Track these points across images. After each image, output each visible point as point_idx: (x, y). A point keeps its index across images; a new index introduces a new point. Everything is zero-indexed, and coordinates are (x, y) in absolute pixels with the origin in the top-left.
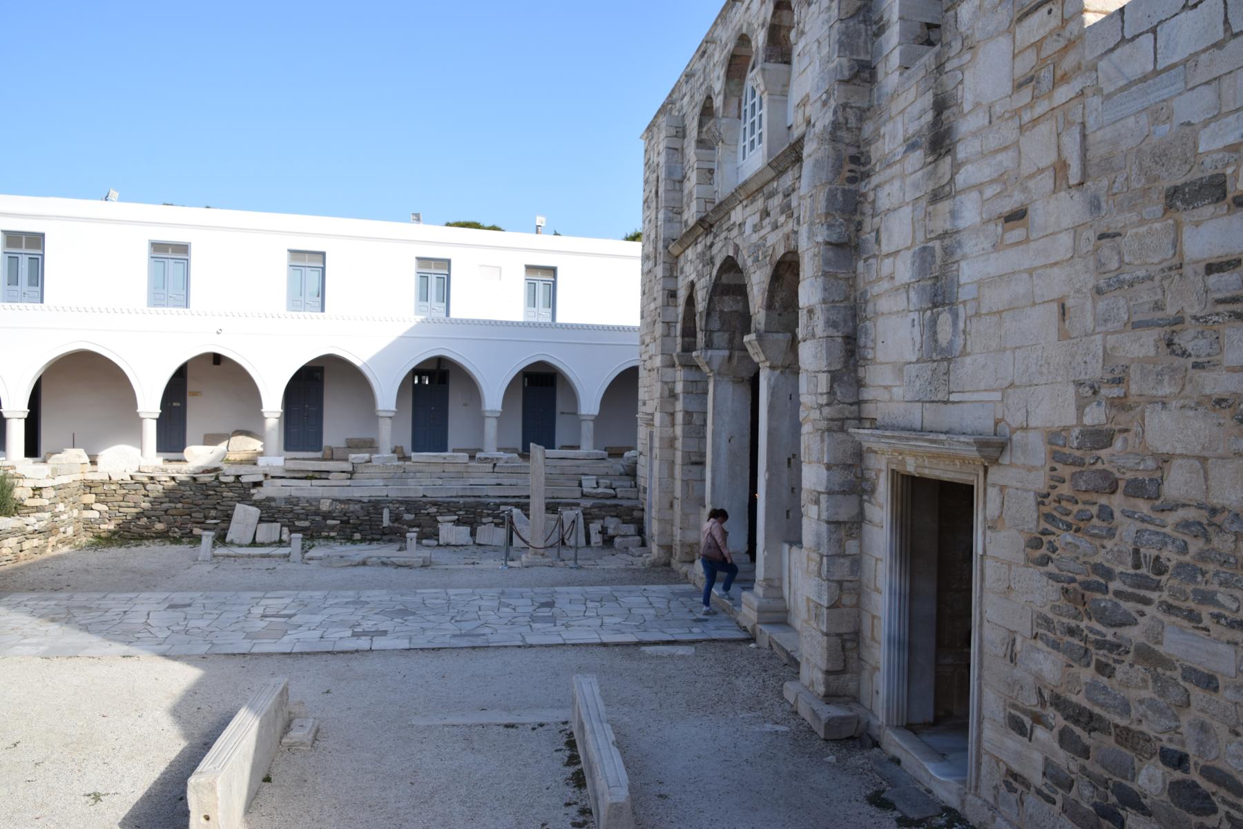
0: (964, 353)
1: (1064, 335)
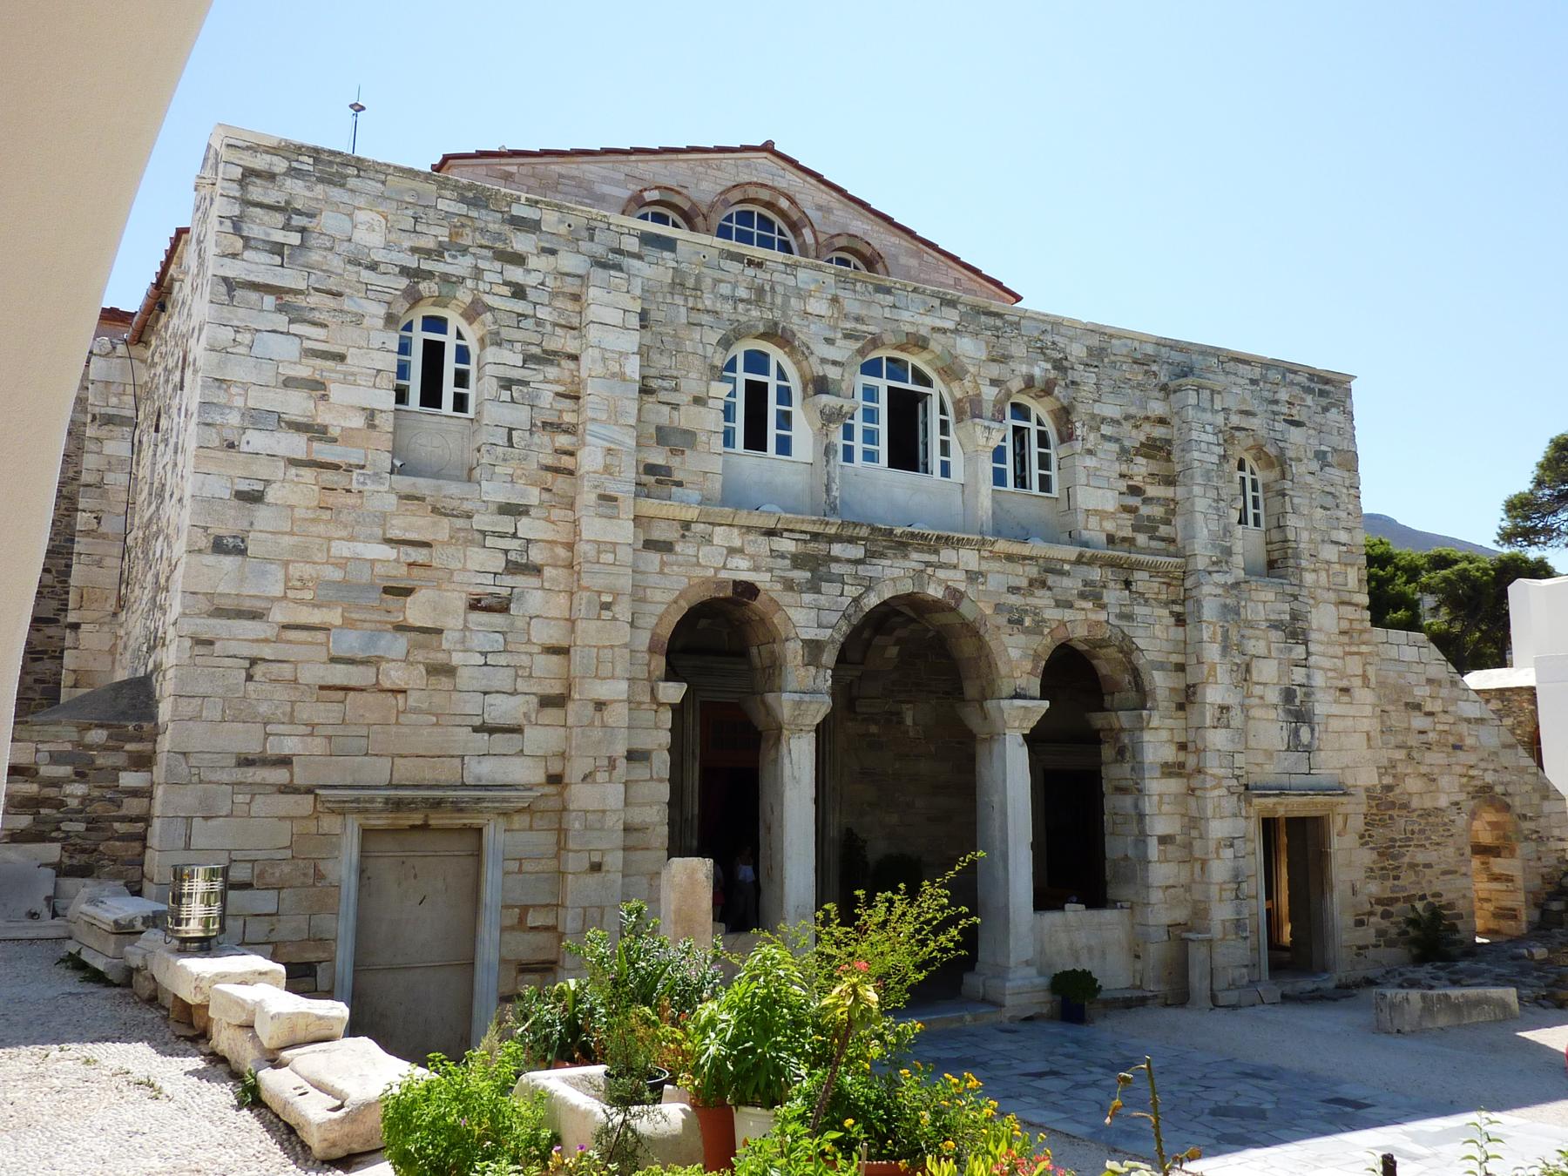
0: (1319, 749)
1: (1370, 747)
